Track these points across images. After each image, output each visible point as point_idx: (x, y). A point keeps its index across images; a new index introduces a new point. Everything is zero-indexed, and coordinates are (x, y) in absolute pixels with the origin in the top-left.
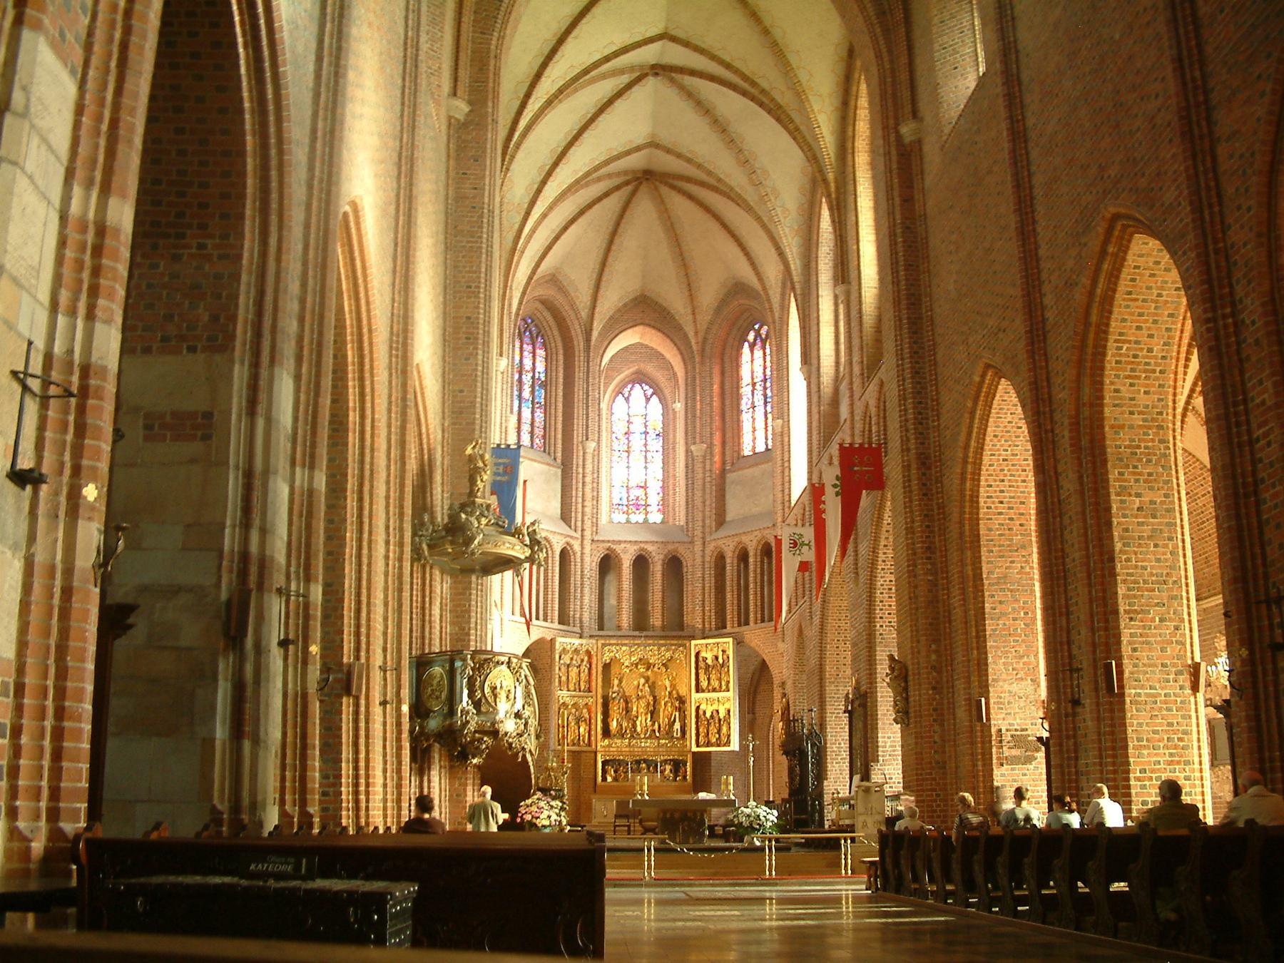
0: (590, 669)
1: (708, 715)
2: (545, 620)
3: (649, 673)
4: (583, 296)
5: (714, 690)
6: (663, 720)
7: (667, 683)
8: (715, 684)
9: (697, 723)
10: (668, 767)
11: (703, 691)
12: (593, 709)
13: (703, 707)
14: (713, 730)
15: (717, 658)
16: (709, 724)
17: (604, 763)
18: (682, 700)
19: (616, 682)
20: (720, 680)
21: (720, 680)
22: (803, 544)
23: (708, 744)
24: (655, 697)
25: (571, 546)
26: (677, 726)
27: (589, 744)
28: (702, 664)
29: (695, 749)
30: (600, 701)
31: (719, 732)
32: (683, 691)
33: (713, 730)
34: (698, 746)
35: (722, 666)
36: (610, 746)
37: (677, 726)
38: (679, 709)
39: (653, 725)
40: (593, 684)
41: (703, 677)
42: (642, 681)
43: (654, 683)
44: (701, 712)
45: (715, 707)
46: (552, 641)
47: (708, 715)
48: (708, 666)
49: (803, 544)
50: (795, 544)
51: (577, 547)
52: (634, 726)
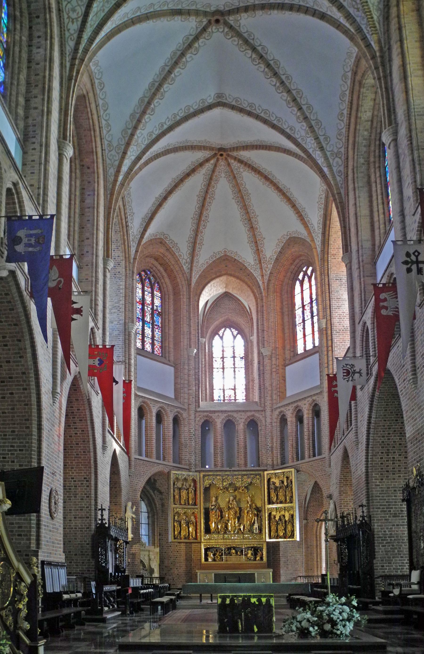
0: (195, 491)
1: (277, 518)
2: (164, 460)
3: (236, 493)
4: (183, 250)
5: (281, 502)
6: (247, 523)
7: (249, 499)
8: (282, 498)
9: (269, 523)
10: (250, 552)
11: (273, 503)
12: (198, 516)
13: (274, 513)
14: (281, 527)
15: (283, 482)
16: (278, 524)
17: (206, 550)
18: (259, 511)
19: (214, 499)
20: (285, 496)
21: (285, 496)
22: (354, 372)
23: (278, 537)
24: (240, 508)
25: (182, 414)
26: (256, 526)
27: (196, 538)
28: (272, 486)
29: (268, 540)
30: (203, 511)
31: (285, 529)
32: (259, 505)
33: (281, 527)
34: (270, 538)
35: (287, 486)
36: (209, 539)
37: (256, 526)
38: (257, 516)
39: (239, 526)
40: (198, 501)
41: (273, 495)
42: (231, 498)
43: (239, 499)
44: (272, 517)
45: (283, 513)
46: (169, 473)
47: (277, 518)
48: (276, 488)
49: (354, 372)
50: (348, 373)
51: (185, 415)
52: (226, 527)
